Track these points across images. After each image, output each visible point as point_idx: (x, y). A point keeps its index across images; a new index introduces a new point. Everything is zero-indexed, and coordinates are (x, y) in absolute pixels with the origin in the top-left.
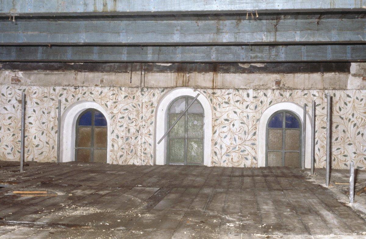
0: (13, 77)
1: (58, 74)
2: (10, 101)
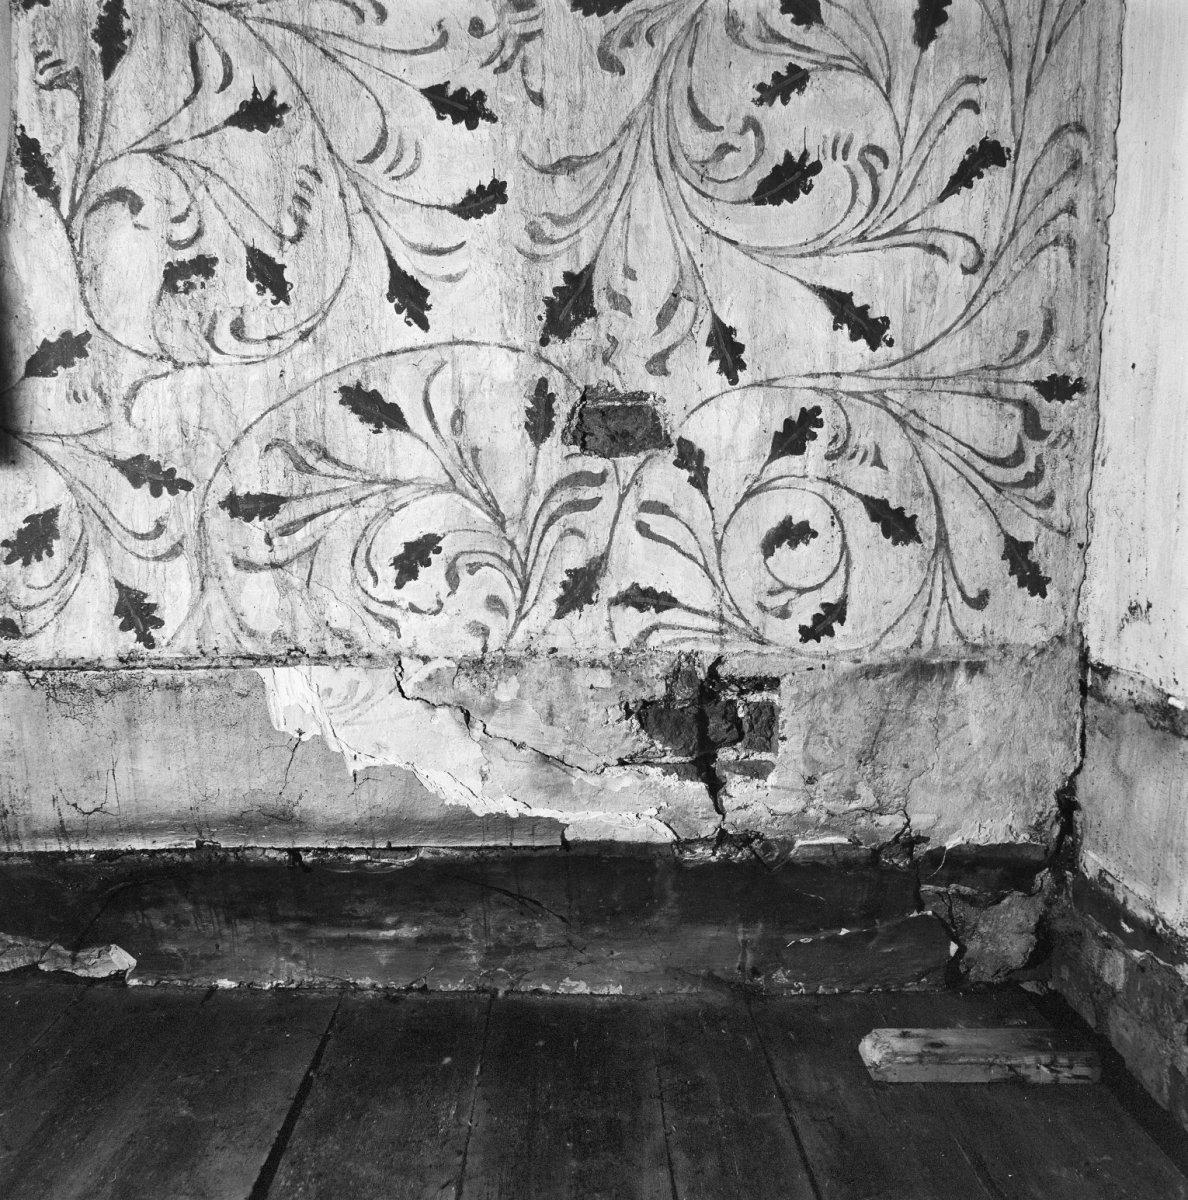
0: (758, 771)
1: (105, 831)
2: (793, 437)
